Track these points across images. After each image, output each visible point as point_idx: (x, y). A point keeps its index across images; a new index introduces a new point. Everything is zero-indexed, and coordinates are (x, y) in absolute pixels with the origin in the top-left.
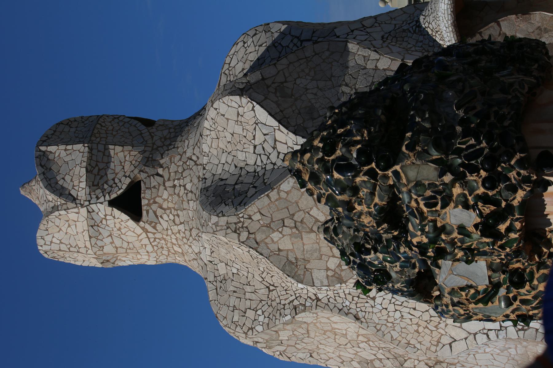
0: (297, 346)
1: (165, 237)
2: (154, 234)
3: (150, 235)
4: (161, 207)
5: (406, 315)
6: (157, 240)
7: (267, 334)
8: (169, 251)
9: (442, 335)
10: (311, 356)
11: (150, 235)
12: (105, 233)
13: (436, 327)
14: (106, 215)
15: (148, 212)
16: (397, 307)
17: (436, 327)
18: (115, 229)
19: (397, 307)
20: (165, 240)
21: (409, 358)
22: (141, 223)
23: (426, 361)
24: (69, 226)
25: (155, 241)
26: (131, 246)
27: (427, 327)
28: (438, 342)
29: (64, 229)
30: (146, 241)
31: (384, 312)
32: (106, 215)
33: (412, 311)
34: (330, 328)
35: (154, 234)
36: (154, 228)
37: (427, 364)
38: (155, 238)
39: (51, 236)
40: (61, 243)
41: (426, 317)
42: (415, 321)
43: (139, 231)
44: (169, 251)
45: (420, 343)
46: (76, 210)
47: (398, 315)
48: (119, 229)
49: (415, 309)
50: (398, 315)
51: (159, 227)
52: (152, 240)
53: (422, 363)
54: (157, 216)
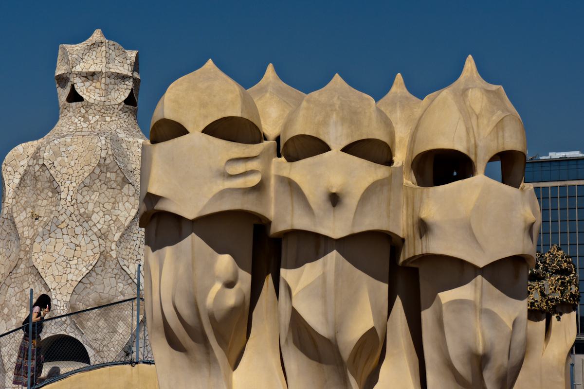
0: (98, 180)
1: (115, 114)
2: (117, 108)
3: (117, 106)
4: (129, 116)
5: (135, 243)
6: (113, 109)
7: (115, 166)
8: (104, 113)
9: (128, 261)
10: (85, 186)
11: (117, 106)
12: (117, 81)
13: (131, 258)
14: (126, 85)
15: (128, 108)
16: (139, 239)
17: (131, 258)
18: (118, 87)
19: (139, 239)
20: (114, 113)
21: (106, 242)
22: (123, 104)
23: (106, 251)
24: (119, 62)
25: (113, 108)
26: (109, 93)
27: (130, 253)
28: (124, 258)
29: (117, 58)
30: (113, 103)
31: (137, 232)
32: (126, 85)
33: (138, 246)
34: (118, 200)
35: (117, 108)
36: (121, 110)
37: (103, 251)
38: (114, 108)
39: (114, 50)
40: (110, 54)
41: (135, 253)
42: (133, 247)
43: (120, 101)
44: (104, 113)
45: (122, 249)
46: (130, 70)
47: (136, 239)
48: (118, 89)
49: (139, 247)
50: (136, 239)
51: (121, 112)
52: (114, 106)
53: (104, 249)
54: (125, 113)
